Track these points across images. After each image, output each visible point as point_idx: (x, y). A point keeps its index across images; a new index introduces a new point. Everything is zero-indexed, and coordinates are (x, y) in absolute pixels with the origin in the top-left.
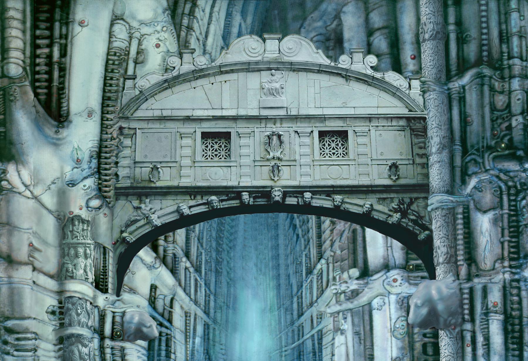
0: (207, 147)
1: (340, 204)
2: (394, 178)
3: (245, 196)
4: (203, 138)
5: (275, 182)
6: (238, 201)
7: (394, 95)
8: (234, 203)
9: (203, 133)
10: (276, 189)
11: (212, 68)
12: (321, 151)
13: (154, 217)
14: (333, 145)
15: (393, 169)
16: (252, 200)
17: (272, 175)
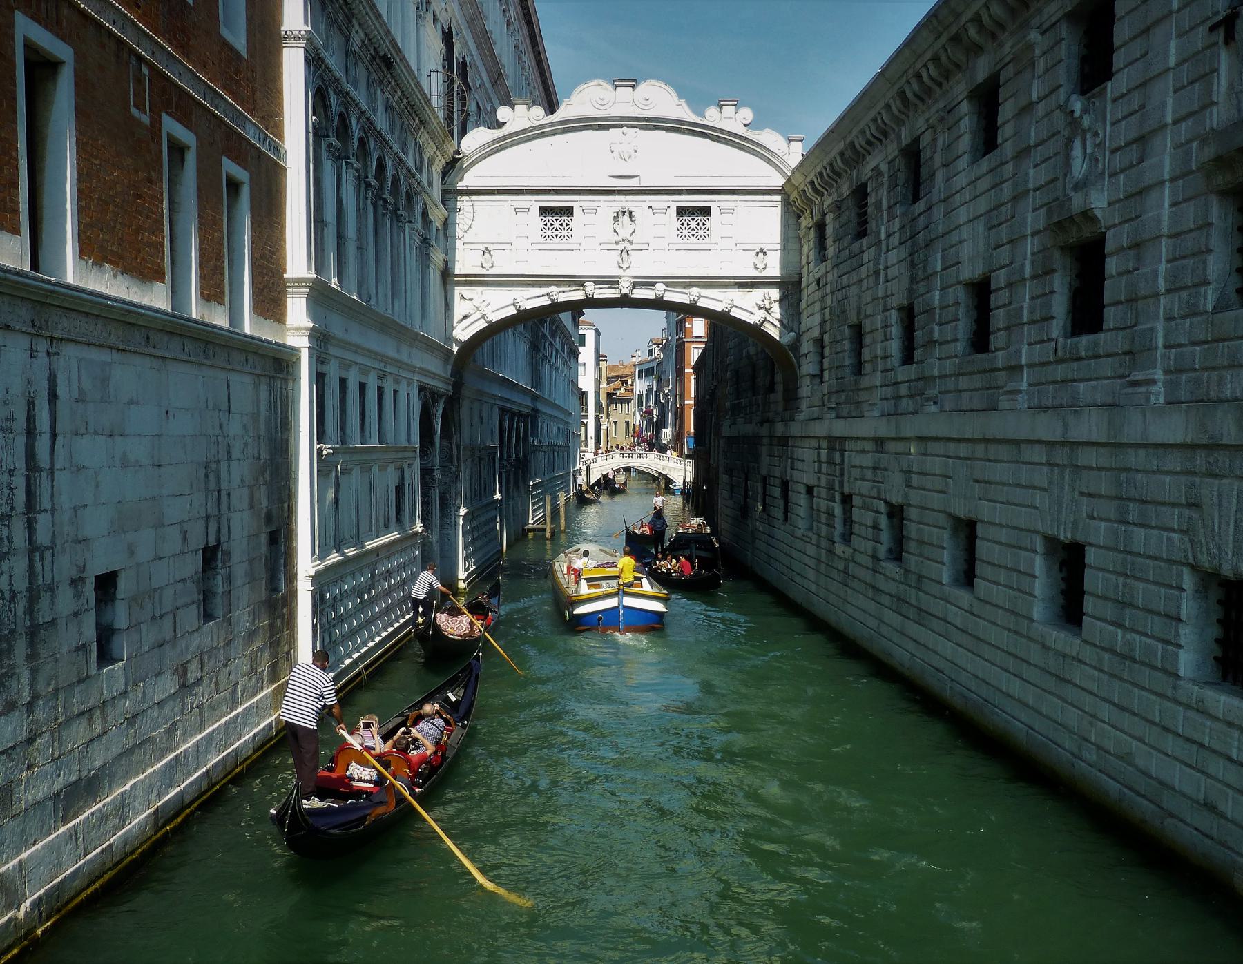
0: (546, 225)
1: (696, 299)
2: (761, 266)
3: (590, 287)
4: (541, 214)
5: (624, 271)
6: (583, 292)
7: (769, 161)
8: (578, 295)
9: (540, 208)
10: (626, 279)
11: (552, 124)
12: (678, 232)
13: (488, 311)
14: (693, 224)
15: (761, 255)
16: (597, 291)
17: (620, 261)
